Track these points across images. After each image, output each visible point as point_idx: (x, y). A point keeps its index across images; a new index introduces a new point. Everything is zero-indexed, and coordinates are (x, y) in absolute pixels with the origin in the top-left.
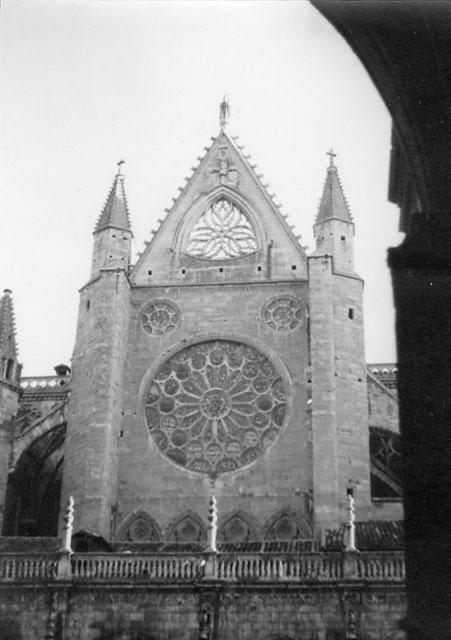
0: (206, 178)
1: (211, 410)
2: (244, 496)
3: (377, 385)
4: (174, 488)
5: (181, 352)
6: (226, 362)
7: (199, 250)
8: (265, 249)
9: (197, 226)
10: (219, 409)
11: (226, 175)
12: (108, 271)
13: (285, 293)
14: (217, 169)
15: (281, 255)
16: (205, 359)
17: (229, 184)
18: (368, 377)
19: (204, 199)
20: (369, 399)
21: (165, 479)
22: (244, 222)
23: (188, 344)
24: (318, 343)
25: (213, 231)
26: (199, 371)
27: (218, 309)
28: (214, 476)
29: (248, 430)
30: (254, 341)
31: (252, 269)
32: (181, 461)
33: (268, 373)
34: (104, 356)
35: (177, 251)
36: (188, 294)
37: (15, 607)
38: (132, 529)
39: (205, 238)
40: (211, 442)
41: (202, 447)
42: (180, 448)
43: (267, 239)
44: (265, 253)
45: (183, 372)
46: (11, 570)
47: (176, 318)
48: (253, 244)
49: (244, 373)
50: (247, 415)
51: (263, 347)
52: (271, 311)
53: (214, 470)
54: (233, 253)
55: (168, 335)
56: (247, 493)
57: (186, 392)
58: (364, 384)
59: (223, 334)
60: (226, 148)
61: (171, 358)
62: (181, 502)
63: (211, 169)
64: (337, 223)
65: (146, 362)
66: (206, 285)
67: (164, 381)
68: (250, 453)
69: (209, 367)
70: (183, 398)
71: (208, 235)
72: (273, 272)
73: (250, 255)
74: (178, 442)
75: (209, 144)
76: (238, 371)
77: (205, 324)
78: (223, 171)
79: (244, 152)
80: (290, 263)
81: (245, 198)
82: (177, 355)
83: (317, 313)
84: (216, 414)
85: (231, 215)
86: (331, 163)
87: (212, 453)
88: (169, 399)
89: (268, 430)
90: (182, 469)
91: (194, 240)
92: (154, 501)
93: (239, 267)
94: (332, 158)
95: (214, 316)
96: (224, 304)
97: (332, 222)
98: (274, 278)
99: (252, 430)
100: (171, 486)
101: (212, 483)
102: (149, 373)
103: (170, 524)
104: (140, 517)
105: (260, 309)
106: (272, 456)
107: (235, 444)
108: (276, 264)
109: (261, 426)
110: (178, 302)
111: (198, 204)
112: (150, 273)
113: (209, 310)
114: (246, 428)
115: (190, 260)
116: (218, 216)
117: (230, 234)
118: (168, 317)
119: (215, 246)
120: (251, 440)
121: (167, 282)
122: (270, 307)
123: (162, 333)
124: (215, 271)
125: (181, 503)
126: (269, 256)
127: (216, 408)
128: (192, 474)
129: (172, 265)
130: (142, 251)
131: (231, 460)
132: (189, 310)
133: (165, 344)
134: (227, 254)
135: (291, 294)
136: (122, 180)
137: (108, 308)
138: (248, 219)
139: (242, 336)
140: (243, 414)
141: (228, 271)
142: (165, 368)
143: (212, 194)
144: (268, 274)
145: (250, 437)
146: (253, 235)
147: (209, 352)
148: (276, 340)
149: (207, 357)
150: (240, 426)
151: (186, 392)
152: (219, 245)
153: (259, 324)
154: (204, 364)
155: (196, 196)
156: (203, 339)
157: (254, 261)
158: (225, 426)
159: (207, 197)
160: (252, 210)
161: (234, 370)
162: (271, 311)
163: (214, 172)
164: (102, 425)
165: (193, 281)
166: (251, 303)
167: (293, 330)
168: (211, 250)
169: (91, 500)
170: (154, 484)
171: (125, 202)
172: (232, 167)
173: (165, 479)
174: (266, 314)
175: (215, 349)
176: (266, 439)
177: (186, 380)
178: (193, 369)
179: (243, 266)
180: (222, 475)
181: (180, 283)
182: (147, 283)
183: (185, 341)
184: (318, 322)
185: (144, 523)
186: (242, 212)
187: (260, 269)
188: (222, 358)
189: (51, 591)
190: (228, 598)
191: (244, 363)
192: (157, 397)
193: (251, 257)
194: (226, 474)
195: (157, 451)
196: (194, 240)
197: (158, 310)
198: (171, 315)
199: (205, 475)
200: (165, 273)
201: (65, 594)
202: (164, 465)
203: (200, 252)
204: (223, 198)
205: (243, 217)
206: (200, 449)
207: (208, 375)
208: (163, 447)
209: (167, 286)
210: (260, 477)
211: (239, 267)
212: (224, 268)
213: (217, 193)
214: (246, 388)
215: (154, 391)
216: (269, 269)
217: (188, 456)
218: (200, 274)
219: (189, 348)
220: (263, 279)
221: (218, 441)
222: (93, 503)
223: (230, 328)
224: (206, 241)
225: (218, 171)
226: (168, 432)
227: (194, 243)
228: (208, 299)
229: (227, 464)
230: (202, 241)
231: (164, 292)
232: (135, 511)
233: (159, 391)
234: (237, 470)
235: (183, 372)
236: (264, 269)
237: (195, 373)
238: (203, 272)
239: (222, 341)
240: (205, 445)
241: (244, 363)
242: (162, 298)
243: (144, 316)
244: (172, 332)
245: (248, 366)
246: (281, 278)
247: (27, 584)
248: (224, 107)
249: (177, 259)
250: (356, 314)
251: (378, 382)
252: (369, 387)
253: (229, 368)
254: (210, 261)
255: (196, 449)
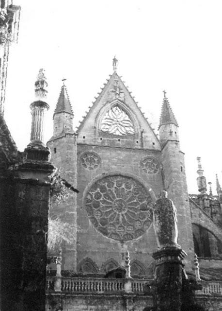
0: (109, 95)
1: (118, 209)
2: (137, 253)
3: (194, 204)
4: (104, 247)
5: (102, 179)
6: (123, 186)
7: (107, 129)
8: (140, 133)
9: (105, 117)
10: (121, 208)
11: (119, 95)
12: (70, 134)
13: (150, 156)
14: (114, 90)
15: (147, 137)
16: (114, 184)
17: (120, 99)
18: (190, 200)
19: (109, 105)
20: (191, 210)
21: (98, 242)
22: (127, 118)
23: (105, 176)
24: (176, 182)
25: (113, 120)
26: (112, 189)
27: (119, 159)
28: (122, 242)
29: (137, 221)
30: (139, 177)
31: (134, 142)
32: (106, 234)
33: (144, 193)
34: (71, 178)
35: (97, 128)
36: (103, 151)
37: (106, 307)
38: (82, 266)
39: (109, 123)
40: (119, 225)
41: (115, 227)
42: (104, 227)
43: (140, 128)
44: (140, 135)
45: (103, 189)
46: (100, 287)
47: (99, 162)
48: (132, 130)
49: (133, 192)
50: (136, 213)
51: (142, 180)
52: (145, 164)
53: (122, 239)
54: (123, 133)
55: (95, 170)
56: (139, 251)
57: (105, 199)
58: (188, 202)
59: (123, 172)
60: (118, 81)
61: (97, 182)
62: (107, 254)
63: (111, 90)
64: (173, 125)
65: (86, 182)
66: (112, 147)
67: (94, 193)
68: (141, 231)
69: (115, 188)
70: (104, 202)
71: (111, 122)
72: (144, 145)
73: (133, 135)
74: (103, 224)
75: (109, 78)
76: (130, 192)
77: (113, 167)
78: (118, 92)
79: (126, 85)
80: (151, 141)
81: (128, 107)
82: (100, 180)
83: (174, 167)
84: (120, 210)
85: (121, 114)
86: (165, 96)
87: (120, 231)
88: (96, 202)
89: (146, 221)
90: (107, 238)
91: (104, 124)
92: (94, 253)
93: (128, 140)
94: (165, 94)
95: (117, 163)
96: (122, 158)
97: (171, 125)
98: (145, 148)
99: (138, 220)
100: (102, 246)
101: (122, 245)
102: (86, 189)
103: (103, 265)
104: (87, 261)
105: (139, 162)
106: (149, 234)
107: (131, 227)
108: (145, 142)
109: (142, 219)
110: (99, 154)
111: (106, 106)
112: (84, 137)
113: (115, 159)
114: (136, 219)
115: (105, 134)
116: (115, 114)
117: (121, 123)
118: (95, 161)
119: (114, 128)
120: (138, 225)
121: (93, 143)
122: (144, 161)
123: (92, 168)
124: (116, 140)
125: (107, 255)
126: (142, 137)
127: (120, 209)
128: (112, 240)
129: (95, 134)
130: (78, 126)
131: (130, 234)
132: (105, 159)
133: (94, 175)
134: (121, 133)
135: (153, 156)
136: (65, 89)
137: (70, 153)
138: (130, 118)
139: (130, 173)
140: (134, 212)
141: (123, 141)
142: (95, 186)
143: (112, 102)
144: (142, 145)
145: (137, 224)
146: (132, 125)
147: (115, 181)
148: (148, 178)
149: (115, 183)
150: (132, 218)
151: (105, 199)
152: (116, 128)
153: (139, 169)
154: (113, 186)
155: (105, 103)
156: (113, 174)
157: (135, 138)
158: (125, 217)
159: (110, 104)
160: (132, 113)
161: (128, 190)
162: (145, 164)
163: (113, 92)
164: (72, 212)
165: (106, 144)
166: (135, 159)
167: (156, 174)
168: (112, 130)
169: (69, 251)
170: (93, 245)
171: (69, 101)
172: (121, 91)
173: (98, 242)
174: (142, 164)
175: (118, 179)
176: (145, 225)
177: (105, 193)
178: (108, 189)
179: (130, 140)
180: (127, 242)
181: (100, 144)
182: (83, 142)
183: (104, 174)
184: (175, 171)
185: (89, 264)
186: (127, 114)
187: (137, 142)
188: (121, 184)
189: (124, 299)
190: (209, 303)
191: (132, 188)
192: (91, 201)
193: (134, 136)
194: (128, 241)
195: (94, 227)
196: (104, 124)
197: (89, 157)
198: (96, 160)
199: (118, 241)
200: (92, 138)
201: (132, 301)
202: (98, 235)
203: (107, 130)
204: (117, 105)
205: (126, 115)
206: (114, 228)
207: (115, 192)
208: (96, 225)
209: (93, 145)
210: (144, 244)
211: (128, 140)
212: (121, 139)
213: (115, 102)
214: (134, 199)
215: (89, 197)
216: (142, 144)
217: (109, 231)
218: (110, 142)
219: (106, 178)
220: (140, 147)
221: (123, 225)
222: (70, 253)
223: (125, 170)
224: (110, 125)
225: (115, 92)
226: (98, 218)
227: (104, 125)
228: (114, 154)
229: (130, 237)
230: (109, 125)
231: (92, 148)
232: (85, 258)
233: (92, 197)
234: (133, 240)
235: (103, 189)
236: (139, 142)
237: (109, 190)
238: (110, 141)
239: (121, 176)
240: (117, 226)
241: (132, 188)
242: (91, 151)
243: (82, 159)
244: (97, 168)
245: (134, 189)
246: (148, 148)
247: (112, 294)
248: (115, 60)
249: (97, 132)
250: (183, 168)
251: (195, 202)
252: (190, 204)
253: (126, 189)
254: (112, 135)
255: (112, 228)
